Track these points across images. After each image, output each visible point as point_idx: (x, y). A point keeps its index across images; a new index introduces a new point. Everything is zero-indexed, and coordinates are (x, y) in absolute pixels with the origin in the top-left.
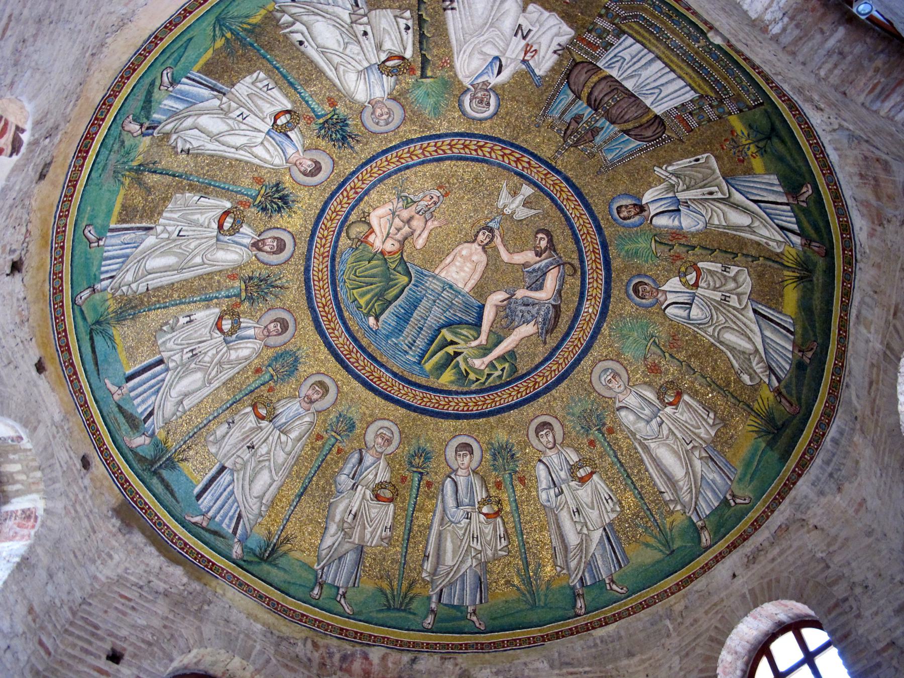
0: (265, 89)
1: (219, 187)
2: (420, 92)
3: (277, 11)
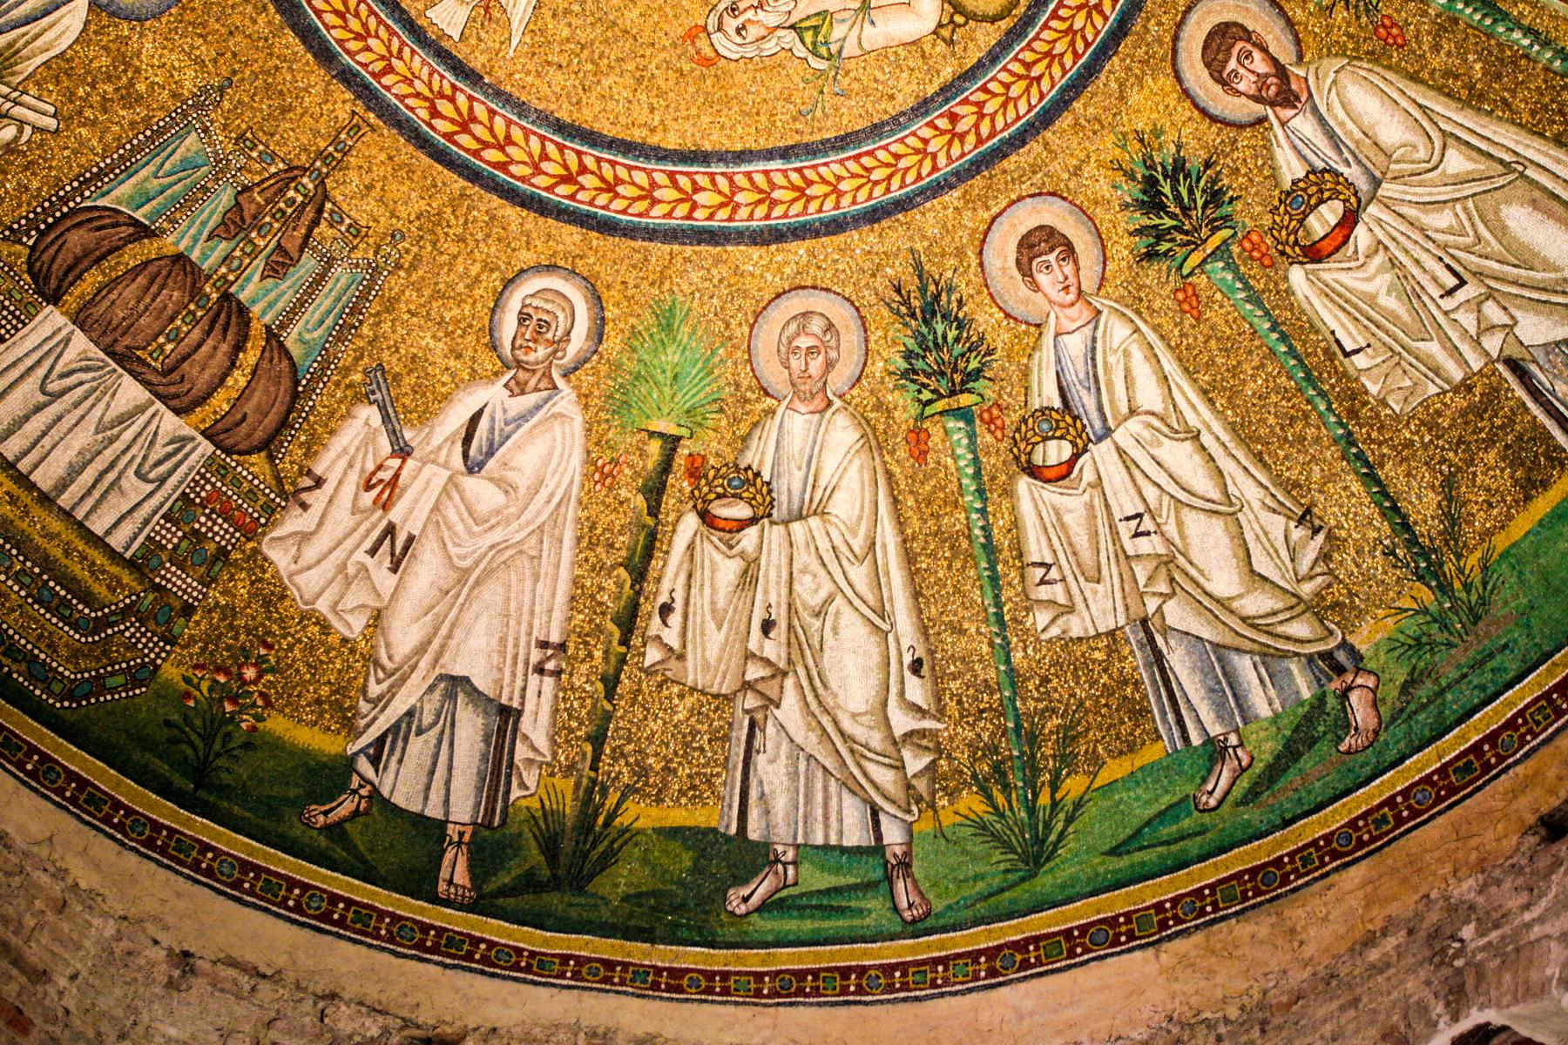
0: (1054, 574)
1: (1292, 351)
2: (692, 394)
3: (919, 799)
